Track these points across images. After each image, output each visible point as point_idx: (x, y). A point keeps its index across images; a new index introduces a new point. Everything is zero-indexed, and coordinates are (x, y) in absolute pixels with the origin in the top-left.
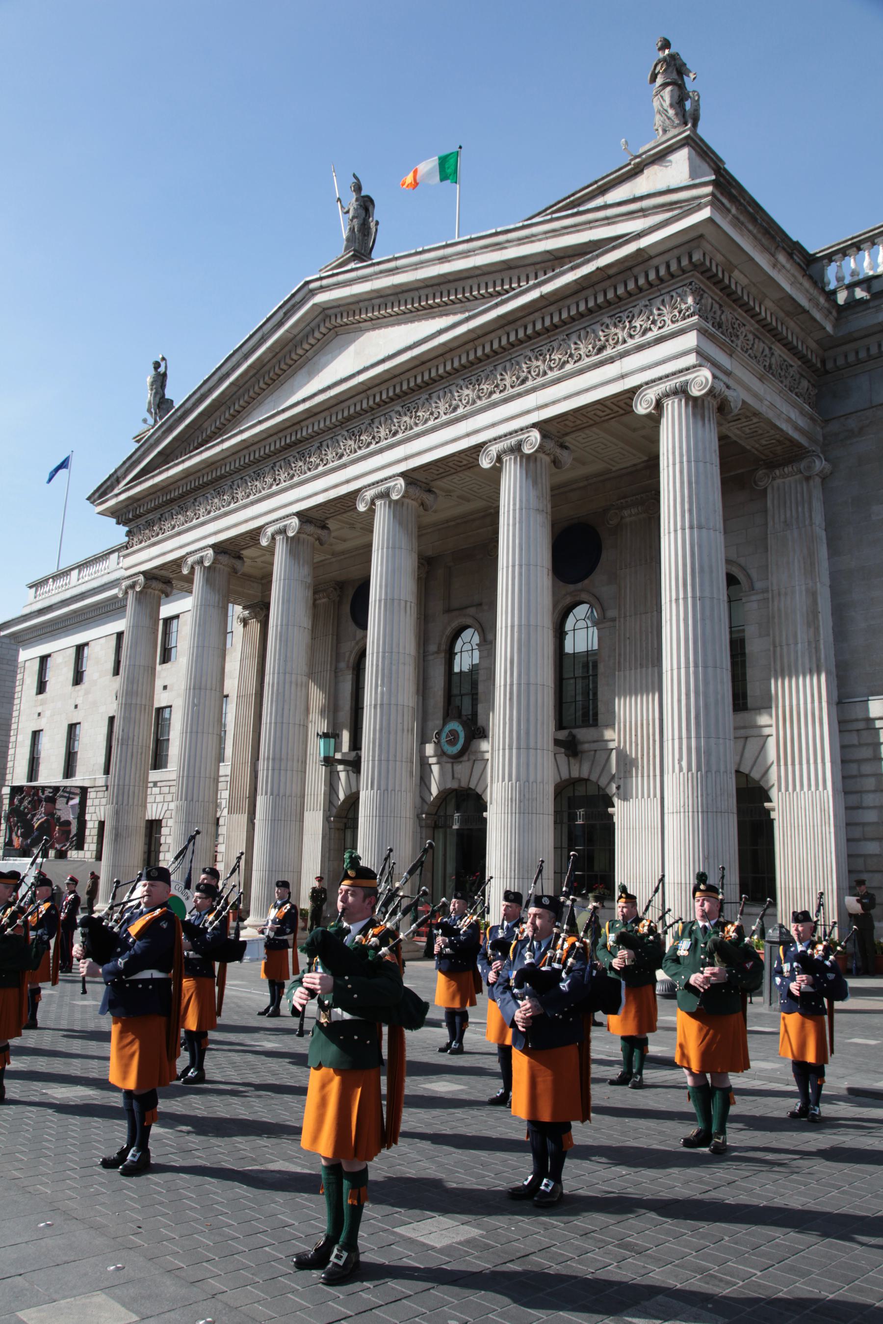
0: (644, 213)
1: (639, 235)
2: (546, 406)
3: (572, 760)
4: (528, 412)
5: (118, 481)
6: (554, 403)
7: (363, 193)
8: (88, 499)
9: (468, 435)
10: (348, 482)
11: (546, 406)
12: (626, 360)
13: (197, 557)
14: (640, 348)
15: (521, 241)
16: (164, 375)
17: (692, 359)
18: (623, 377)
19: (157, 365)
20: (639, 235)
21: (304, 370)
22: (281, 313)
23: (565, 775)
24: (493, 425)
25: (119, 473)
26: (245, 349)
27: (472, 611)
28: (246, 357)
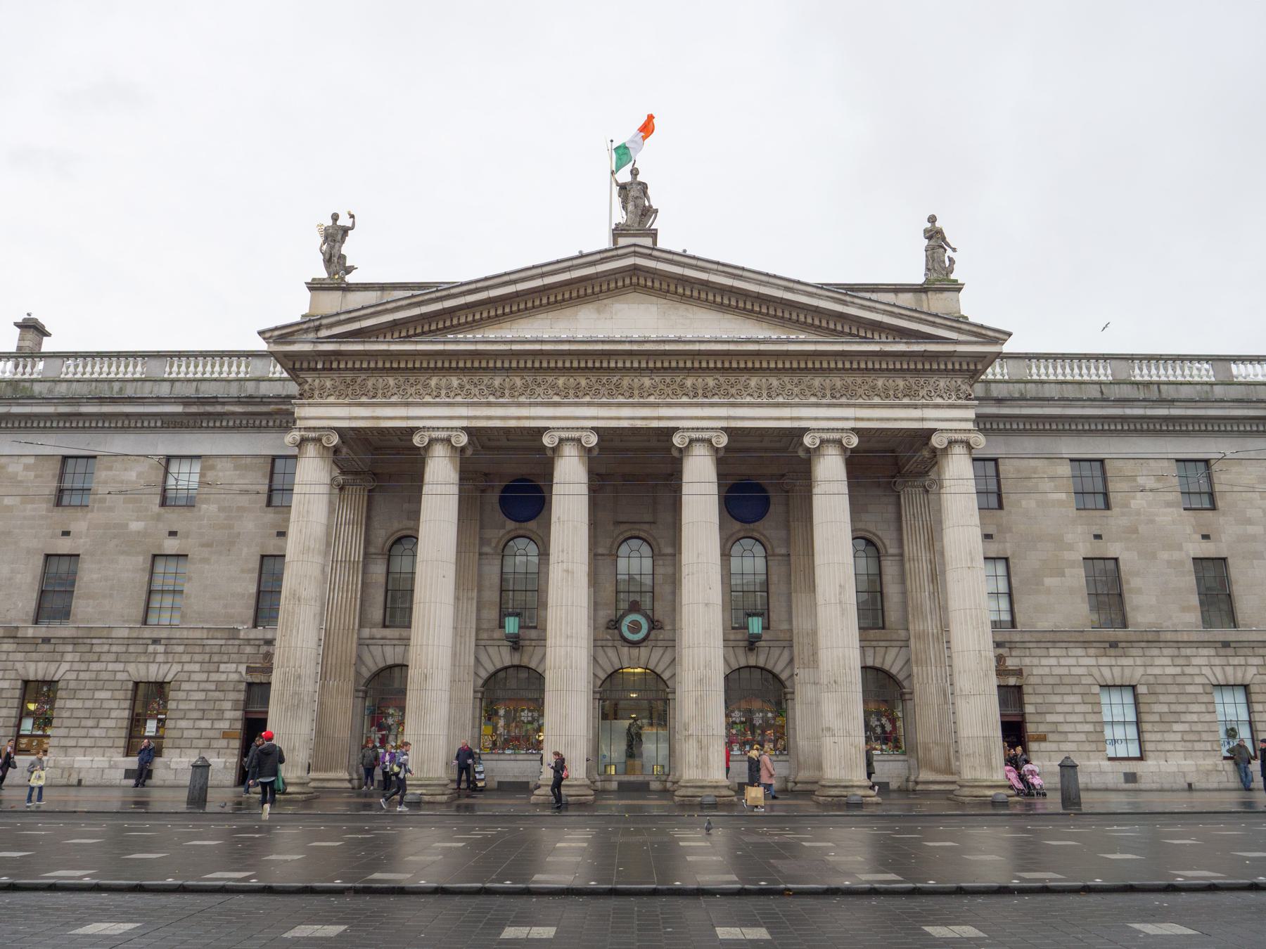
0: (959, 330)
1: (957, 342)
2: (862, 419)
3: (749, 654)
4: (847, 419)
5: (318, 329)
6: (869, 419)
7: (639, 178)
8: (260, 333)
9: (791, 419)
10: (659, 418)
11: (862, 419)
12: (925, 410)
13: (443, 434)
14: (937, 406)
15: (862, 307)
16: (345, 231)
17: (970, 426)
18: (923, 419)
19: (335, 217)
20: (957, 342)
21: (590, 306)
22: (598, 257)
23: (743, 663)
24: (816, 419)
25: (324, 322)
26: (545, 269)
27: (646, 527)
28: (543, 275)
